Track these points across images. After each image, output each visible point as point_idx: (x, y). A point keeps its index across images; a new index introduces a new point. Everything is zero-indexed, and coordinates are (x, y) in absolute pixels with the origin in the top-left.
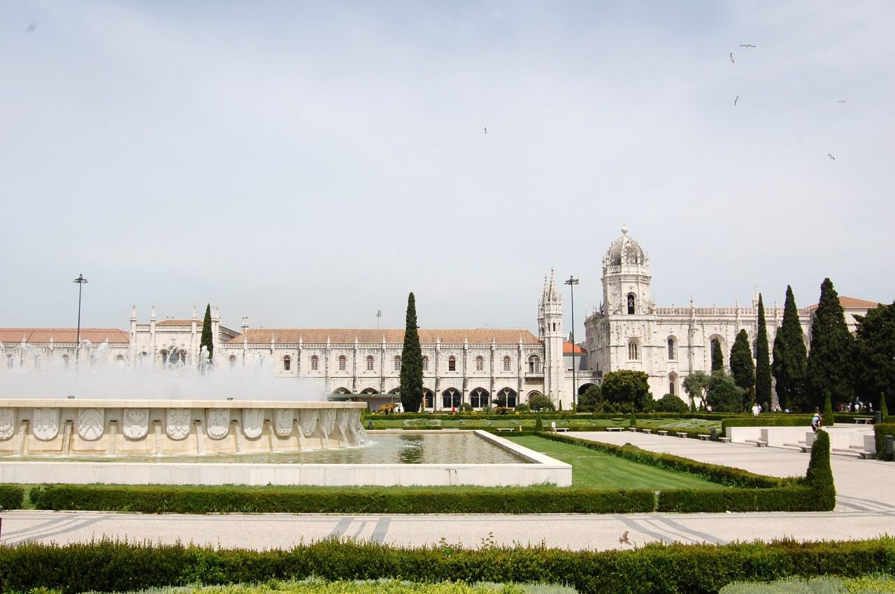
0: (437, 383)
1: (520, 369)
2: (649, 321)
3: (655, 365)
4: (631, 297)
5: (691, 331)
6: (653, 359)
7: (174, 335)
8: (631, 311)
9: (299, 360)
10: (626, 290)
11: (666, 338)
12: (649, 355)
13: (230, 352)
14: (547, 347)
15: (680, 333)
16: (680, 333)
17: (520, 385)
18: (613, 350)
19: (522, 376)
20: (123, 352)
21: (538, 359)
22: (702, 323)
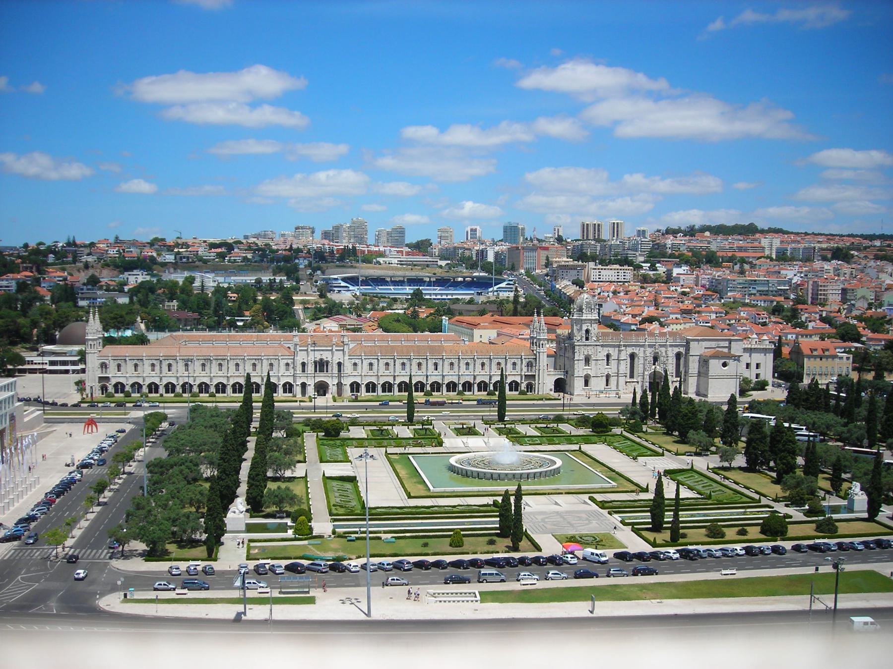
0: (475, 379)
1: (521, 370)
2: (597, 345)
3: (598, 370)
4: (587, 331)
5: (620, 351)
6: (599, 367)
7: (322, 352)
8: (587, 339)
9: (395, 365)
10: (585, 327)
11: (605, 354)
12: (596, 364)
13: (353, 361)
14: (537, 357)
15: (614, 352)
16: (614, 352)
17: (521, 379)
18: (576, 362)
19: (523, 374)
20: (290, 361)
21: (532, 364)
22: (625, 346)
